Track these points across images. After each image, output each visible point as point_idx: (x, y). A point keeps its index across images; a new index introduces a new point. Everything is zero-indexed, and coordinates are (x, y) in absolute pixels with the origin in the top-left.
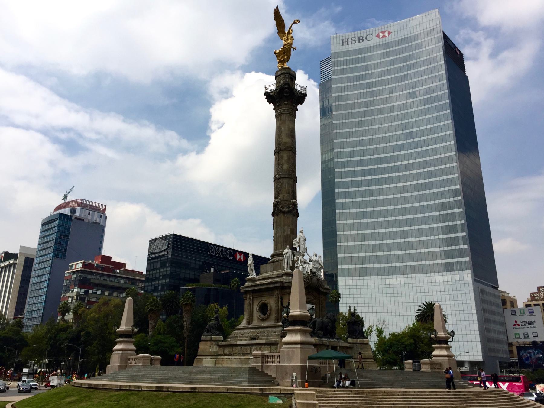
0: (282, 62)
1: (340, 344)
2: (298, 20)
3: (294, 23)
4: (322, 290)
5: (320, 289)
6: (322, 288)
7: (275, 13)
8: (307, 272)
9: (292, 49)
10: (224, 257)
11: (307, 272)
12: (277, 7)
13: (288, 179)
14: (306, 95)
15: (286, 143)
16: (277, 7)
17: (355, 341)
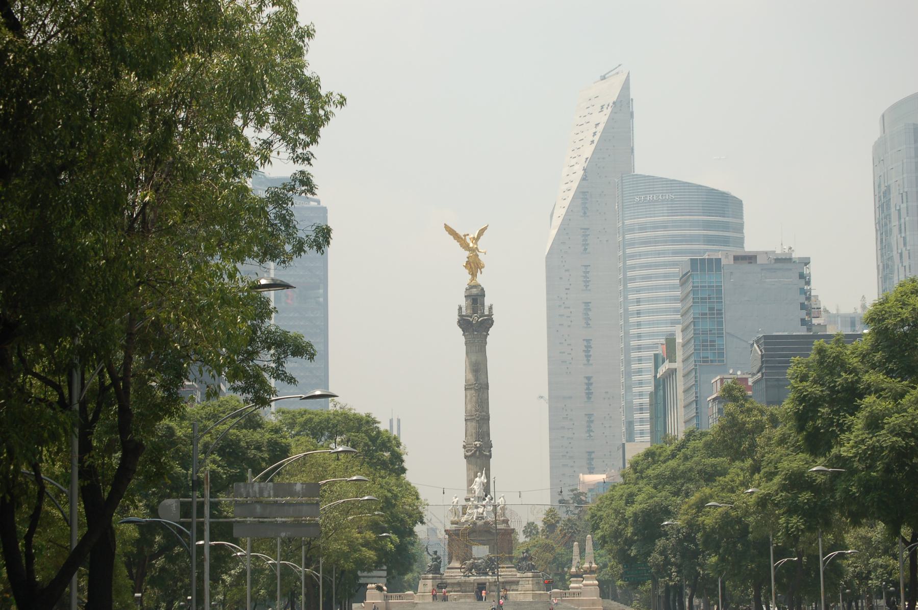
0: (474, 275)
14: (490, 315)
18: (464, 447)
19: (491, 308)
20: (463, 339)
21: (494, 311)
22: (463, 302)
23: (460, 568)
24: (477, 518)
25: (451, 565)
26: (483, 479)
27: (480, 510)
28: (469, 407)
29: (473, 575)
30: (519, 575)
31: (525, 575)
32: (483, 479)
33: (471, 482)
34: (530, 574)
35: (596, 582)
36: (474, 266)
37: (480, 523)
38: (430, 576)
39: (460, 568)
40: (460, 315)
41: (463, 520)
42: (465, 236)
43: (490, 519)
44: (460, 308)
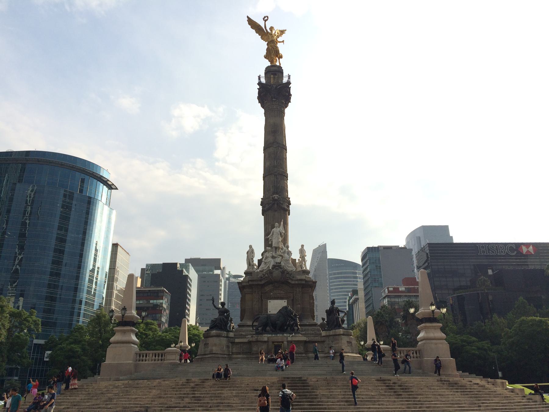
0: (271, 61)
1: (289, 339)
2: (265, 17)
3: (266, 21)
4: (293, 282)
5: (290, 281)
6: (292, 280)
7: (249, 24)
8: (269, 267)
9: (279, 45)
10: (503, 254)
11: (269, 267)
12: (248, 17)
14: (289, 83)
16: (248, 17)
17: (328, 333)
18: (262, 204)
19: (289, 77)
20: (262, 111)
21: (292, 81)
22: (263, 75)
24: (274, 267)
25: (243, 322)
26: (281, 228)
27: (278, 260)
28: (268, 164)
29: (268, 333)
30: (324, 333)
33: (267, 233)
35: (444, 335)
36: (273, 53)
37: (276, 273)
38: (214, 332)
39: (252, 326)
40: (260, 84)
42: (266, 19)
43: (290, 268)
44: (259, 78)
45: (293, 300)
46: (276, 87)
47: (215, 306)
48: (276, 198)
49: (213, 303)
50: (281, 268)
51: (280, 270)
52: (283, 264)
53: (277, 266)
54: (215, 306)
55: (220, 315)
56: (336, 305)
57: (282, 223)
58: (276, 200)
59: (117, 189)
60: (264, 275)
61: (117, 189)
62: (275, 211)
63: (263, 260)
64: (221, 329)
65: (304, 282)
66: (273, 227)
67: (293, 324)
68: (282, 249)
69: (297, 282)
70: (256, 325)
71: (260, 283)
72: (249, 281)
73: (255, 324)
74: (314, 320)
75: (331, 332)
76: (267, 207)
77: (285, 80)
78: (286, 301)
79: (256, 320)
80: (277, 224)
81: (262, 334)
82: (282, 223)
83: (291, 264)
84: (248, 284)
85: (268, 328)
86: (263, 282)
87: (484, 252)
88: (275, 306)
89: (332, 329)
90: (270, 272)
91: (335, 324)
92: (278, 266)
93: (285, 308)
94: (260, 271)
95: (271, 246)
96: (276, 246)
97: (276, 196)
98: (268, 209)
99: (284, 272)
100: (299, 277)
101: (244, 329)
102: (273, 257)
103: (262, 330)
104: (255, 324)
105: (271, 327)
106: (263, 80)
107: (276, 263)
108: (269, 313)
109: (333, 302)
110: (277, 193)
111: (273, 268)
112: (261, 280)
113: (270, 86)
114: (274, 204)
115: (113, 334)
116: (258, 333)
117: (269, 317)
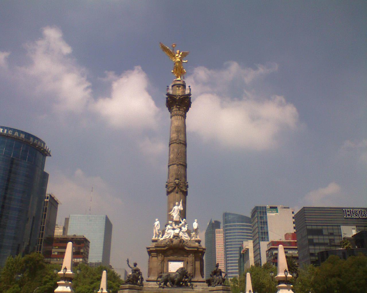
5: (186, 248)
10: (364, 217)
11: (170, 237)
13: (172, 166)
14: (190, 94)
15: (172, 138)
16: (160, 43)
18: (167, 186)
23: (157, 281)
24: (174, 236)
25: (150, 279)
26: (181, 207)
27: (177, 231)
28: (172, 156)
31: (215, 288)
32: (181, 207)
34: (220, 287)
37: (176, 241)
38: (127, 286)
40: (168, 94)
41: (162, 239)
43: (185, 237)
45: (187, 262)
46: (179, 98)
47: (129, 266)
48: (177, 183)
49: (128, 263)
50: (179, 238)
51: (179, 239)
52: (181, 234)
53: (176, 236)
54: (129, 266)
55: (133, 273)
56: (220, 267)
57: (181, 202)
58: (177, 184)
59: (50, 156)
60: (167, 243)
61: (50, 156)
62: (177, 193)
63: (166, 230)
64: (133, 284)
65: (196, 249)
66: (175, 205)
67: (188, 280)
68: (181, 223)
69: (191, 249)
70: (159, 281)
71: (163, 249)
72: (156, 247)
73: (159, 279)
74: (203, 277)
75: (215, 288)
76: (170, 189)
77: (187, 92)
78: (183, 263)
79: (160, 277)
80: (177, 203)
81: (163, 288)
82: (181, 202)
83: (187, 235)
84: (154, 249)
85: (168, 283)
86: (166, 248)
87: (349, 215)
88: (174, 267)
89: (215, 286)
90: (171, 241)
91: (218, 282)
92: (177, 236)
93: (182, 269)
94: (164, 240)
95: (172, 220)
96: (176, 220)
97: (177, 181)
98: (172, 191)
99: (182, 241)
100: (193, 245)
101: (150, 283)
102: (174, 229)
103: (164, 284)
104: (159, 279)
105: (171, 283)
106: (171, 92)
107: (176, 233)
108: (169, 272)
109: (217, 266)
110: (178, 179)
111: (173, 238)
112: (164, 247)
113: (175, 96)
114: (175, 188)
115: (56, 286)
116: (160, 287)
117: (169, 274)
